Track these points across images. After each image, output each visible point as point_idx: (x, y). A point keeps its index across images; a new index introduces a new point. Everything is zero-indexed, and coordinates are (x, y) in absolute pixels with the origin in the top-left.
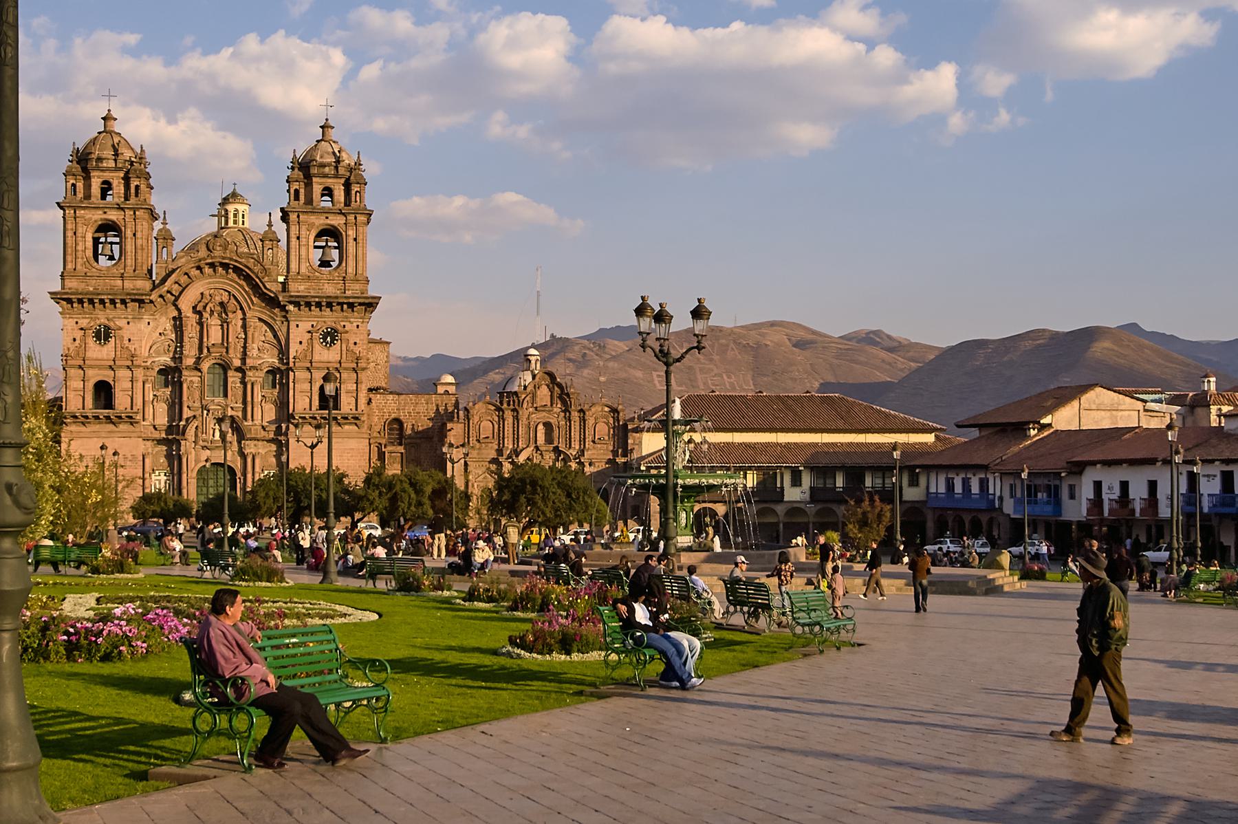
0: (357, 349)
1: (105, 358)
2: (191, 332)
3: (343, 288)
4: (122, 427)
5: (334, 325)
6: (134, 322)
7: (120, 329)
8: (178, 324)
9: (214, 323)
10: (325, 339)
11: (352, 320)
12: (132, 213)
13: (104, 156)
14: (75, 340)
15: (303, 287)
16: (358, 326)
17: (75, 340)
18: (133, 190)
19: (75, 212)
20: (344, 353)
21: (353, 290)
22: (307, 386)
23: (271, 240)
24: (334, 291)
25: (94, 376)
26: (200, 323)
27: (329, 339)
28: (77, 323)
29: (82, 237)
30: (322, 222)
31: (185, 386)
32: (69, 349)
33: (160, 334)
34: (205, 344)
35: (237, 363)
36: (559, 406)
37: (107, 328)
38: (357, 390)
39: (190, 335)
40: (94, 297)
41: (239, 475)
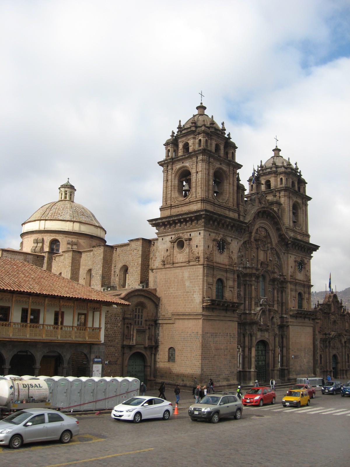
0: (308, 274)
1: (222, 263)
4: (229, 314)
11: (307, 257)
12: (232, 168)
19: (209, 158)
22: (293, 293)
28: (210, 234)
41: (271, 348)
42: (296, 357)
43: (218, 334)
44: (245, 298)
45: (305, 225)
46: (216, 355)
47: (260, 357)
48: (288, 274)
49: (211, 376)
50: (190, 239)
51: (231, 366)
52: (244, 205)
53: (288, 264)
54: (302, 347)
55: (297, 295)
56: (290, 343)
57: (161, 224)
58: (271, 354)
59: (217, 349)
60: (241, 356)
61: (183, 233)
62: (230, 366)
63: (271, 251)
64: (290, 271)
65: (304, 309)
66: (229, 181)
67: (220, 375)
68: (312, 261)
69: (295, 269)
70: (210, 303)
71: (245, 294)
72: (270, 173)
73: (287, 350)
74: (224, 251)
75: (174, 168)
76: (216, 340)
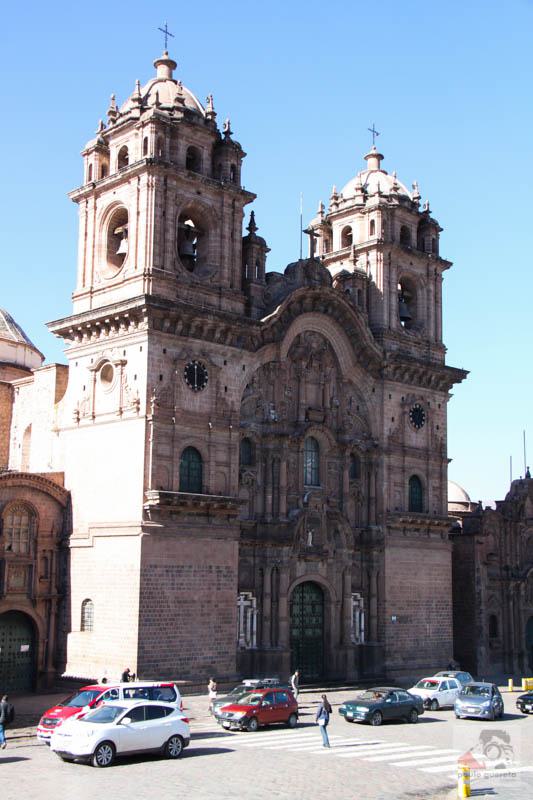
0: (440, 435)
6: (232, 364)
14: (161, 377)
16: (439, 406)
17: (161, 377)
22: (397, 478)
28: (165, 351)
31: (284, 465)
42: (401, 619)
43: (186, 569)
44: (265, 492)
45: (432, 325)
46: (179, 615)
47: (307, 620)
48: (382, 434)
49: (165, 660)
50: (123, 363)
51: (221, 639)
52: (265, 283)
53: (382, 413)
54: (420, 597)
55: (407, 482)
56: (387, 588)
57: (71, 331)
58: (334, 611)
59: (179, 602)
60: (255, 617)
61: (112, 350)
62: (216, 640)
63: (338, 383)
64: (388, 427)
65: (427, 512)
66: (222, 230)
67: (188, 659)
68: (451, 405)
69: (402, 421)
70: (158, 501)
71: (265, 482)
72: (350, 212)
73: (379, 605)
74: (203, 386)
75: (99, 206)
76: (180, 582)
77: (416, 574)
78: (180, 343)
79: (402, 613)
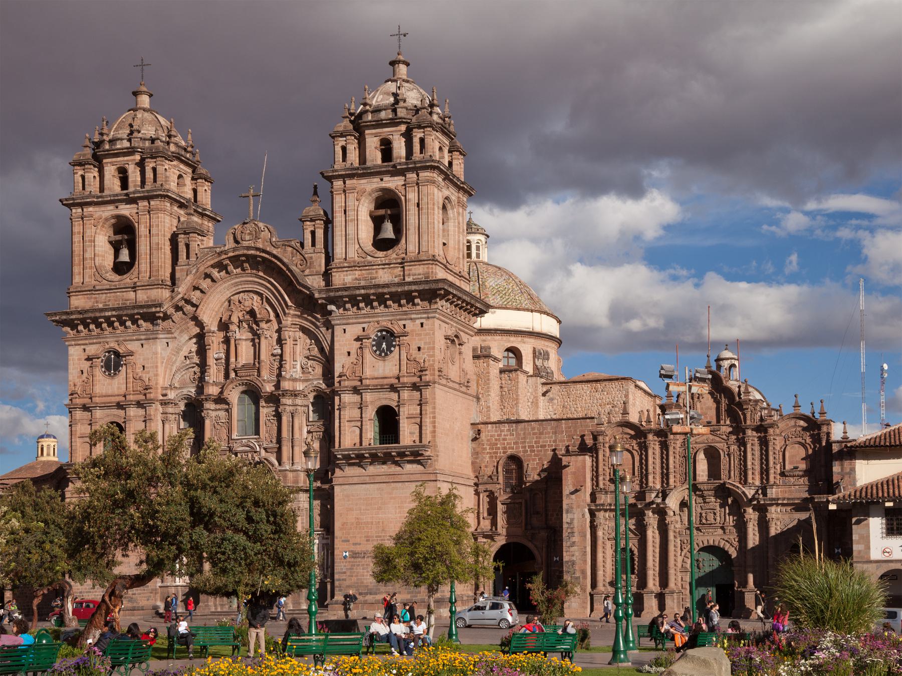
0: (420, 357)
1: (116, 393)
2: (215, 351)
3: (402, 273)
5: (390, 326)
7: (131, 354)
8: (201, 339)
9: (242, 335)
10: (379, 345)
11: (413, 316)
13: (119, 136)
15: (350, 277)
16: (422, 324)
18: (149, 174)
20: (404, 362)
21: (416, 272)
22: (356, 413)
23: (312, 220)
24: (390, 278)
25: (102, 417)
26: (227, 341)
27: (384, 345)
28: (84, 350)
29: (90, 241)
30: (375, 186)
31: (208, 423)
32: (75, 385)
33: (185, 357)
34: (232, 366)
35: (269, 388)
36: (728, 422)
37: (117, 354)
38: (421, 414)
39: (216, 356)
40: (98, 314)
77: (380, 508)
78: (95, 341)
79: (358, 549)
